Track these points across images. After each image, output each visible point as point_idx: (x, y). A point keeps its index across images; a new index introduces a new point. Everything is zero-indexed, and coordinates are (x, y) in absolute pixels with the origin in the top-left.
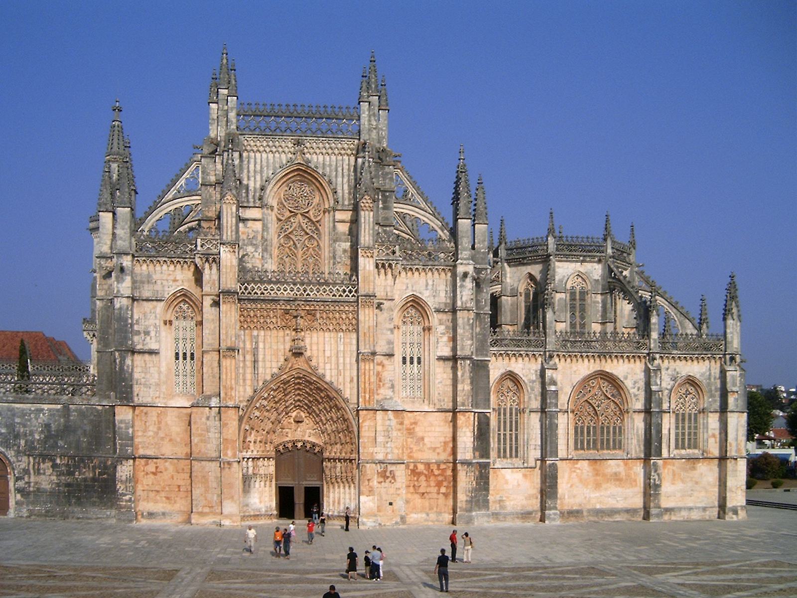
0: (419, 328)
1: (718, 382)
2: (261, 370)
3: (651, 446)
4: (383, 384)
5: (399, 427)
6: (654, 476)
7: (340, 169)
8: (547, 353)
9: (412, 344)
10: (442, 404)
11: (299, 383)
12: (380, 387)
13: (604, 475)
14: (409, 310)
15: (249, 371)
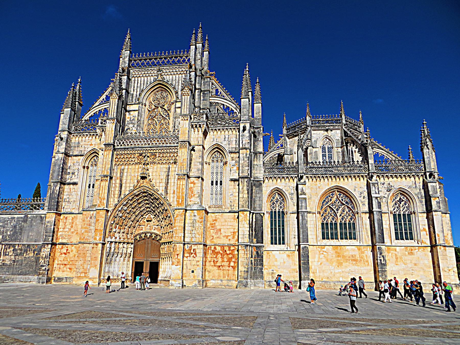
0: (222, 164)
1: (422, 191)
2: (123, 188)
3: (376, 235)
4: (194, 195)
5: (200, 220)
6: (379, 257)
7: (180, 82)
8: (299, 175)
9: (217, 173)
10: (233, 208)
11: (145, 196)
12: (192, 197)
13: (344, 256)
14: (216, 153)
15: (118, 189)
